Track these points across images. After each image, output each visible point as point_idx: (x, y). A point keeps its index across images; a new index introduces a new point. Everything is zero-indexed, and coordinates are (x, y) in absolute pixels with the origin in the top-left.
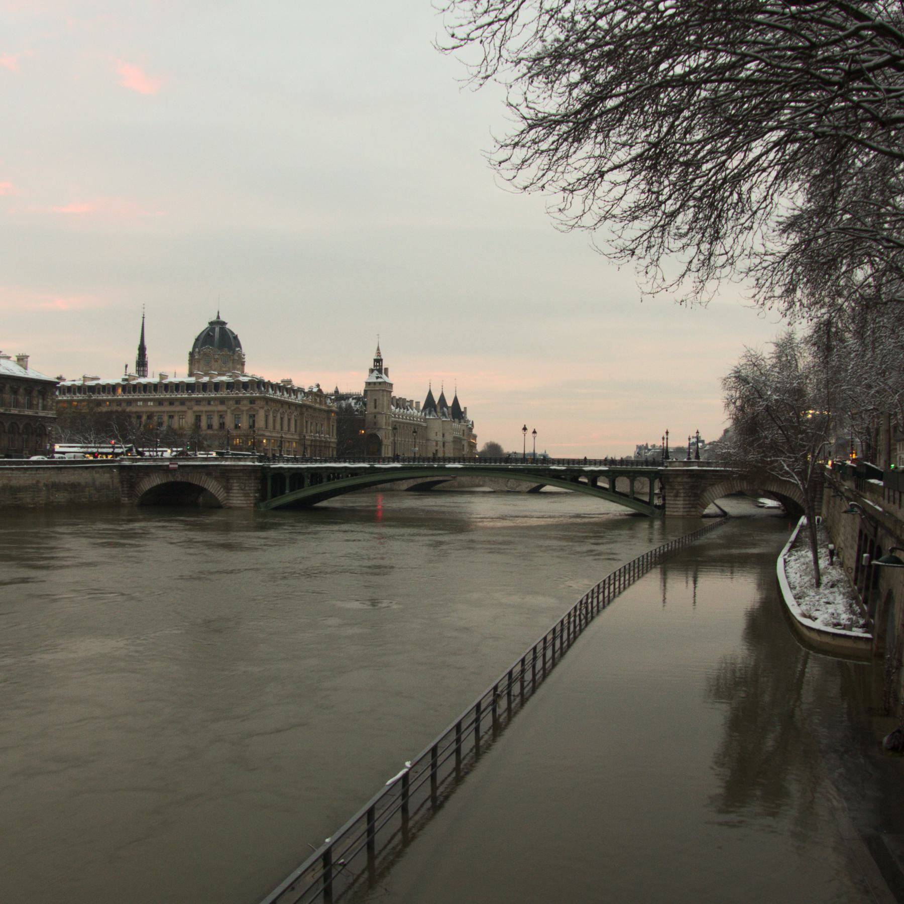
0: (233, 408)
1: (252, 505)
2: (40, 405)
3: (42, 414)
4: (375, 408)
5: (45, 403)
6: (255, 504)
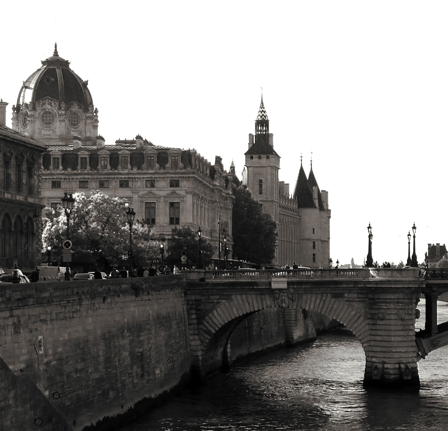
0: (141, 193)
1: (414, 344)
3: (30, 200)
4: (261, 193)
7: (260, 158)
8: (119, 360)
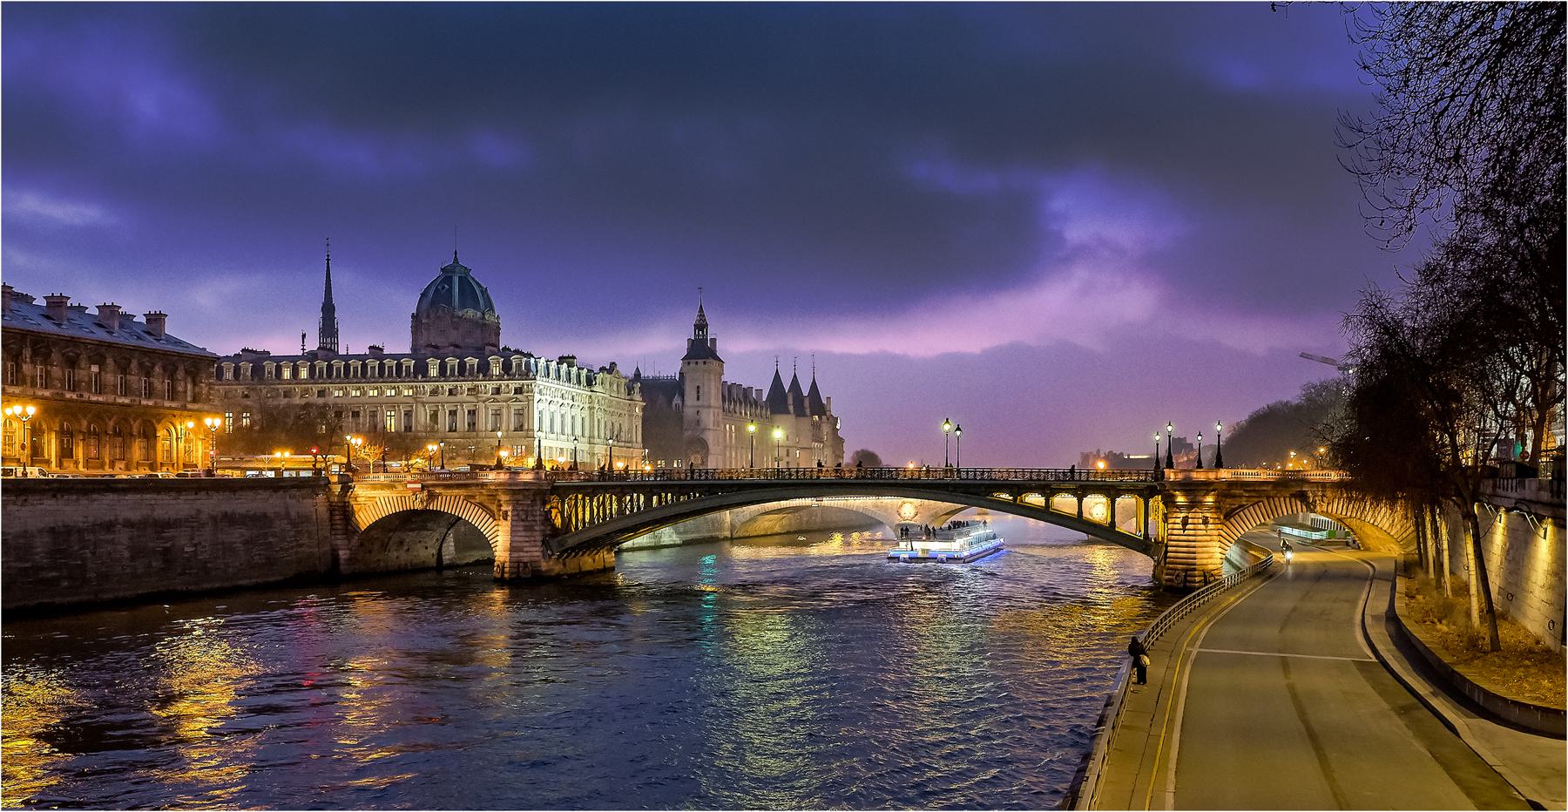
2: (189, 393)
4: (698, 399)
5: (197, 389)
6: (543, 542)
7: (697, 363)
8: (93, 553)
